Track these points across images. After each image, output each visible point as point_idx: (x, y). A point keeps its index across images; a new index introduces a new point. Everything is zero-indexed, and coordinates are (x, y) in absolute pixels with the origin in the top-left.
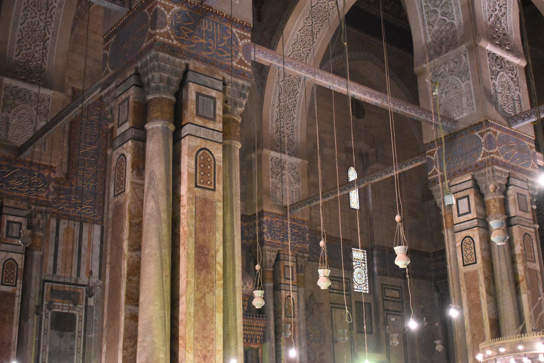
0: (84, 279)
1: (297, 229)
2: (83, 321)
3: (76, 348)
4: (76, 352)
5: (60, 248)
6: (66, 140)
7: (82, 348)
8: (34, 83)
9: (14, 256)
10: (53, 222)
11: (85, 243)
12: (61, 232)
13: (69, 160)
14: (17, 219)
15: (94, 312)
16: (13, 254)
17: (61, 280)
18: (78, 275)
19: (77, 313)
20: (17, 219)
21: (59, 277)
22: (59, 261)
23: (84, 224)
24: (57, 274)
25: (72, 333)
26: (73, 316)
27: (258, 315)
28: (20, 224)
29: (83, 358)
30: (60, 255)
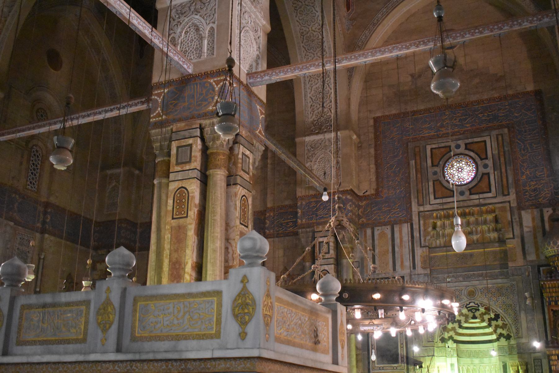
1: (374, 211)
6: (373, 162)
9: (326, 267)
10: (369, 231)
11: (397, 241)
12: (376, 237)
13: (377, 178)
16: (325, 266)
17: (380, 276)
18: (394, 269)
21: (378, 274)
23: (395, 226)
27: (548, 275)
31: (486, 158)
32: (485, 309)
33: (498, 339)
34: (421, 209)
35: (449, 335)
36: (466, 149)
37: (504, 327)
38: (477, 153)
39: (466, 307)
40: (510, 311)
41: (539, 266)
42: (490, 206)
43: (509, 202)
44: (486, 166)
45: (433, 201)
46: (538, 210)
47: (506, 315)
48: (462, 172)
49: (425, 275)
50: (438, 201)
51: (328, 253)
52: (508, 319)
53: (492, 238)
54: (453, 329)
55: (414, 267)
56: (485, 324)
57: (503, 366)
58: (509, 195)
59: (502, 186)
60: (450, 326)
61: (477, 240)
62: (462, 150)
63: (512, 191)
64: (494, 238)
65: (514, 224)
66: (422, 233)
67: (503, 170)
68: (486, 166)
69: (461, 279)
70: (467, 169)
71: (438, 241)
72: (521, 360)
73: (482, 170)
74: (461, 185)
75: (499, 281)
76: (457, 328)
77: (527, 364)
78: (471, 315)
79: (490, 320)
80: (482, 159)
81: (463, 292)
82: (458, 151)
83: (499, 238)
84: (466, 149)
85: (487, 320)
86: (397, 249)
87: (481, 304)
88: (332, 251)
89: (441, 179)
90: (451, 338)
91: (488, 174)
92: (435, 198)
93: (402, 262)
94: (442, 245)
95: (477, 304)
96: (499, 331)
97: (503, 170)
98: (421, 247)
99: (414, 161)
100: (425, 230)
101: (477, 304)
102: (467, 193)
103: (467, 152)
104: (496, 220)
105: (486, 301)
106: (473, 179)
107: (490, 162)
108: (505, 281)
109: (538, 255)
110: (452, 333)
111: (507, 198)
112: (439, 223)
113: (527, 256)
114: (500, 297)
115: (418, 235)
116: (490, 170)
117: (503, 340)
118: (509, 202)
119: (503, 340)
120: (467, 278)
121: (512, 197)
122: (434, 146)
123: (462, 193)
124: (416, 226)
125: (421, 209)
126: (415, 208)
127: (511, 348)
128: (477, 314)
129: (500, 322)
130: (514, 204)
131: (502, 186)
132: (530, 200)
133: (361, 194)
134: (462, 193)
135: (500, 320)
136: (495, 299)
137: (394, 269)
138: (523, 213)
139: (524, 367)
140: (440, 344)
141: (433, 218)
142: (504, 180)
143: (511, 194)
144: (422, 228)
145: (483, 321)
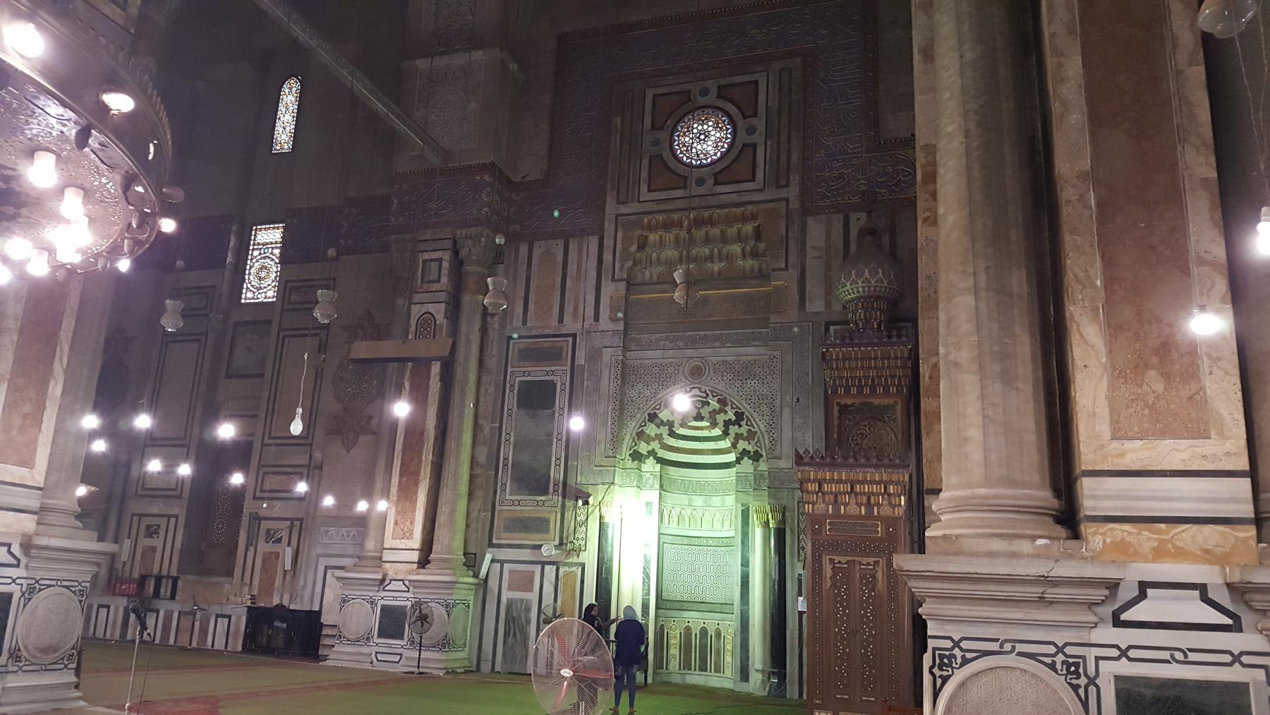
0: (570, 326)
5: (533, 286)
8: (456, 51)
9: (431, 308)
10: (524, 249)
11: (572, 267)
14: (436, 255)
17: (534, 333)
18: (561, 320)
19: (557, 379)
20: (436, 255)
21: (531, 329)
22: (531, 307)
24: (529, 325)
26: (552, 385)
28: (440, 260)
30: (532, 296)
31: (755, 115)
32: (719, 401)
33: (738, 461)
34: (624, 209)
35: (650, 448)
36: (718, 96)
37: (750, 436)
38: (735, 104)
40: (764, 407)
41: (828, 325)
42: (750, 207)
43: (787, 200)
44: (751, 131)
45: (645, 195)
46: (841, 216)
47: (755, 415)
48: (705, 141)
49: (615, 332)
50: (656, 196)
51: (438, 281)
53: (748, 268)
54: (659, 437)
55: (597, 319)
56: (717, 432)
58: (787, 186)
59: (778, 169)
60: (651, 430)
61: (720, 273)
62: (711, 98)
63: (795, 178)
64: (752, 269)
65: (791, 242)
66: (618, 255)
67: (784, 138)
68: (751, 131)
70: (715, 135)
71: (647, 273)
72: (772, 501)
73: (743, 137)
74: (701, 166)
75: (751, 350)
76: (665, 436)
77: (784, 510)
79: (727, 424)
80: (745, 117)
82: (702, 100)
83: (760, 269)
84: (718, 96)
85: (721, 424)
86: (569, 283)
88: (444, 279)
89: (666, 154)
90: (652, 453)
91: (754, 146)
92: (649, 191)
93: (576, 308)
94: (655, 279)
96: (742, 445)
97: (784, 138)
98: (613, 280)
99: (619, 119)
100: (625, 249)
102: (711, 181)
103: (720, 103)
104: (758, 235)
105: (720, 387)
106: (724, 155)
107: (760, 123)
108: (761, 350)
109: (828, 305)
110: (655, 445)
111: (783, 193)
112: (653, 237)
113: (807, 304)
115: (611, 258)
116: (758, 138)
118: (787, 200)
120: (692, 343)
121: (793, 191)
122: (660, 91)
123: (700, 182)
124: (608, 243)
125: (624, 209)
126: (611, 209)
127: (758, 477)
129: (744, 430)
130: (794, 205)
131: (778, 169)
132: (828, 197)
133: (517, 179)
134: (700, 182)
135: (743, 423)
136: (738, 384)
137: (561, 320)
138: (810, 220)
139: (779, 516)
140: (630, 464)
141: (642, 228)
142: (784, 157)
143: (792, 184)
144: (619, 245)
145: (714, 424)
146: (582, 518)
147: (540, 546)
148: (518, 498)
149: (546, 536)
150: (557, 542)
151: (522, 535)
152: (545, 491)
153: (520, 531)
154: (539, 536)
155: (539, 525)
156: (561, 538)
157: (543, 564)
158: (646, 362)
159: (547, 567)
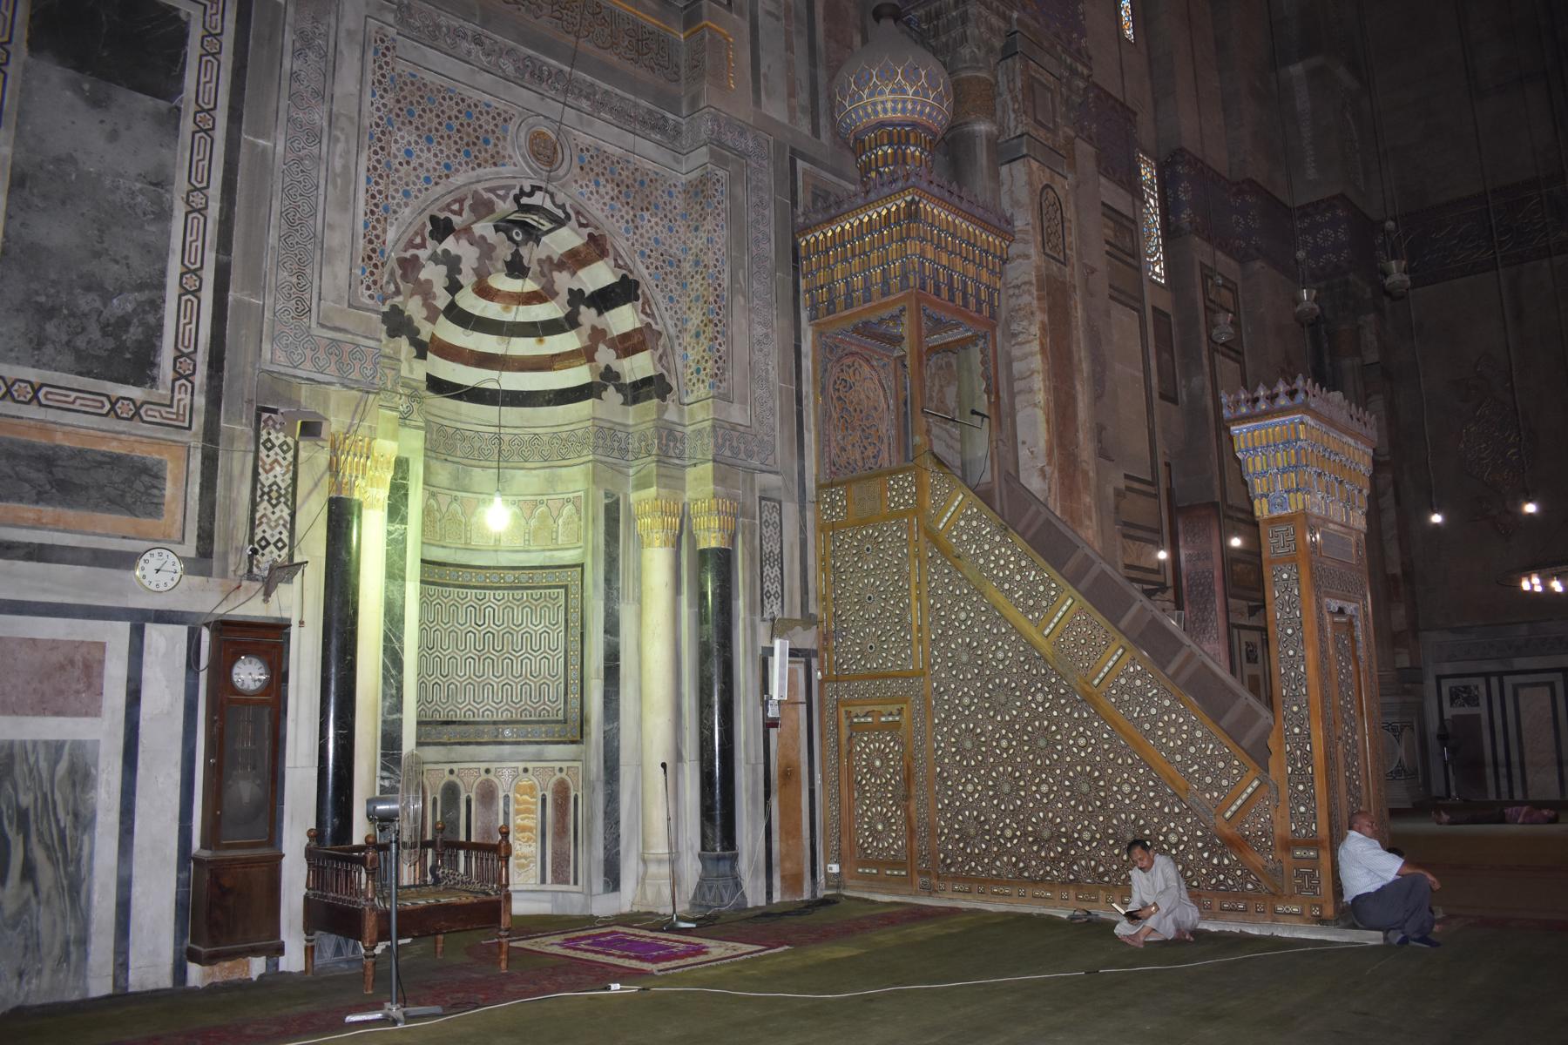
2: (227, 58)
3: (181, 184)
4: (179, 210)
7: (215, 190)
15: (289, 37)
25: (163, 105)
29: (224, 244)
39: (517, 199)
52: (667, 315)
57: (608, 508)
69: (510, 69)
78: (505, 251)
81: (512, 127)
85: (564, 296)
87: (578, 213)
95: (563, 207)
101: (563, 207)
105: (596, 209)
114: (647, 215)
117: (612, 395)
119: (612, 395)
128: (532, 255)
129: (623, 319)
146: (278, 475)
147: (128, 561)
148: (33, 375)
149: (146, 523)
150: (190, 549)
151: (48, 512)
152: (140, 368)
153: (40, 498)
154: (122, 521)
155: (128, 486)
156: (206, 537)
157: (139, 620)
158: (429, 77)
159: (153, 632)
